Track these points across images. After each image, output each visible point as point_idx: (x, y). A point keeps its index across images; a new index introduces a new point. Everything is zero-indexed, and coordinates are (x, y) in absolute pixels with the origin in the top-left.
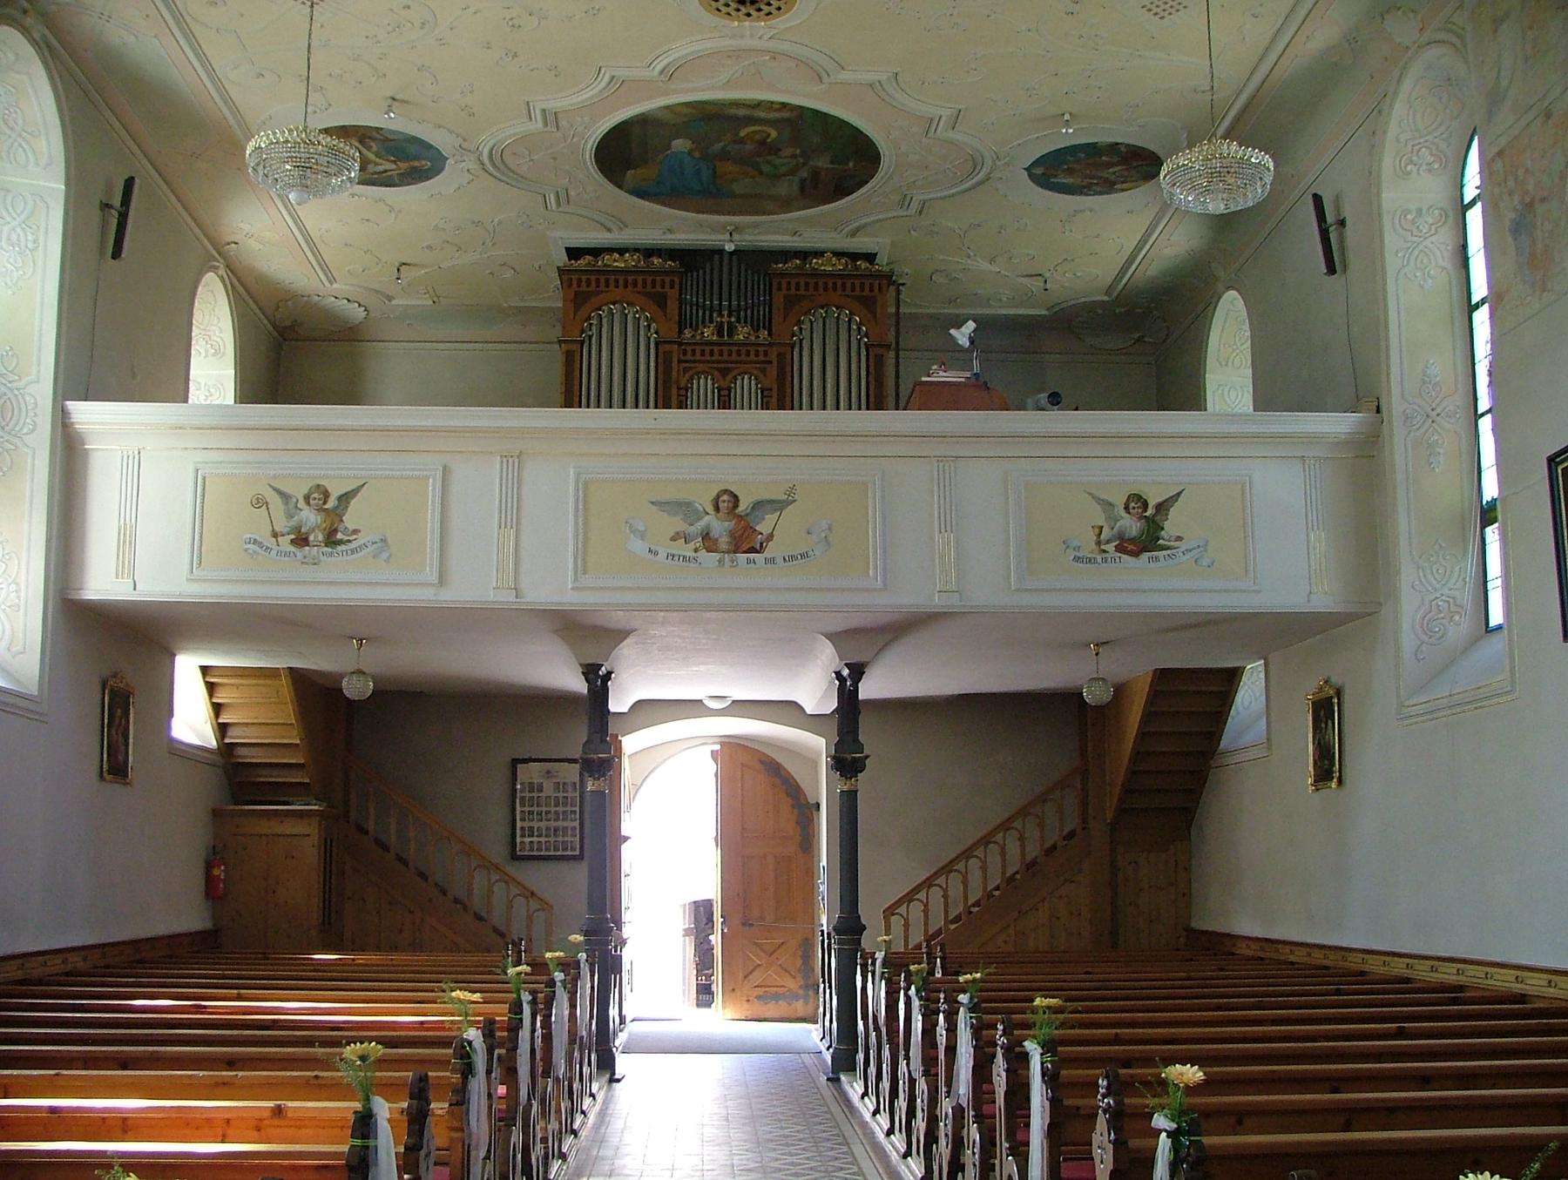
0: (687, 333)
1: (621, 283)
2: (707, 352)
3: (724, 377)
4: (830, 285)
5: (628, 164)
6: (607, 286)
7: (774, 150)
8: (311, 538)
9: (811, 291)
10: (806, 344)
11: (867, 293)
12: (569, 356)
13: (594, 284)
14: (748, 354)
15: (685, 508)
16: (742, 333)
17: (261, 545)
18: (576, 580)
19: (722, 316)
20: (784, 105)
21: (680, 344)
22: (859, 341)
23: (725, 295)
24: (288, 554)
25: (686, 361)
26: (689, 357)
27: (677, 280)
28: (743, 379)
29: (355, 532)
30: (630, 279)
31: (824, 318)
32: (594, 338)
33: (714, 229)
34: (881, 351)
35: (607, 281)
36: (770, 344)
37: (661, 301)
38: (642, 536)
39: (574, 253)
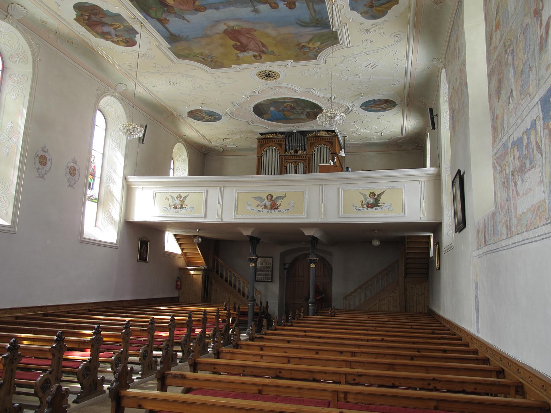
0: (287, 153)
1: (271, 141)
2: (291, 157)
3: (296, 163)
13: (265, 142)
14: (299, 157)
16: (300, 152)
19: (295, 148)
21: (285, 155)
22: (329, 152)
23: (296, 143)
25: (286, 160)
27: (284, 140)
28: (300, 163)
30: (273, 140)
31: (320, 147)
32: (265, 155)
35: (268, 141)
36: (307, 155)
37: (280, 145)
39: (261, 134)
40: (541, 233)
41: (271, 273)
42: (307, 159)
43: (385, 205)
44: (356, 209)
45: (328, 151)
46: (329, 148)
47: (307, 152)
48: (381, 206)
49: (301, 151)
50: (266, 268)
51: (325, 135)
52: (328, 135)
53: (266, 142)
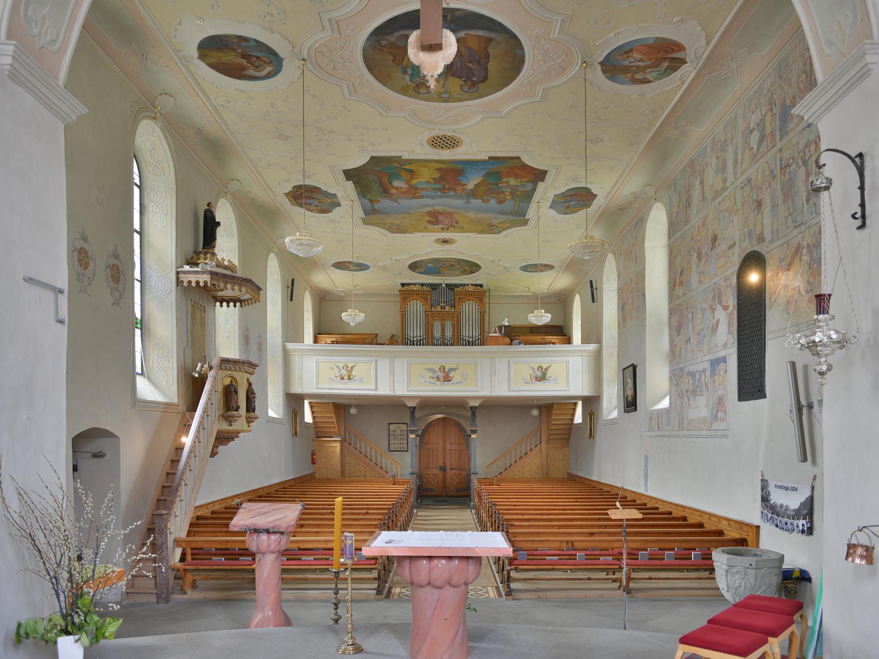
7: (453, 266)
8: (344, 378)
10: (464, 311)
15: (432, 370)
16: (447, 308)
18: (408, 388)
19: (442, 303)
20: (455, 259)
29: (355, 376)
34: (484, 313)
37: (426, 299)
38: (422, 377)
40: (704, 434)
42: (455, 317)
45: (477, 308)
46: (478, 305)
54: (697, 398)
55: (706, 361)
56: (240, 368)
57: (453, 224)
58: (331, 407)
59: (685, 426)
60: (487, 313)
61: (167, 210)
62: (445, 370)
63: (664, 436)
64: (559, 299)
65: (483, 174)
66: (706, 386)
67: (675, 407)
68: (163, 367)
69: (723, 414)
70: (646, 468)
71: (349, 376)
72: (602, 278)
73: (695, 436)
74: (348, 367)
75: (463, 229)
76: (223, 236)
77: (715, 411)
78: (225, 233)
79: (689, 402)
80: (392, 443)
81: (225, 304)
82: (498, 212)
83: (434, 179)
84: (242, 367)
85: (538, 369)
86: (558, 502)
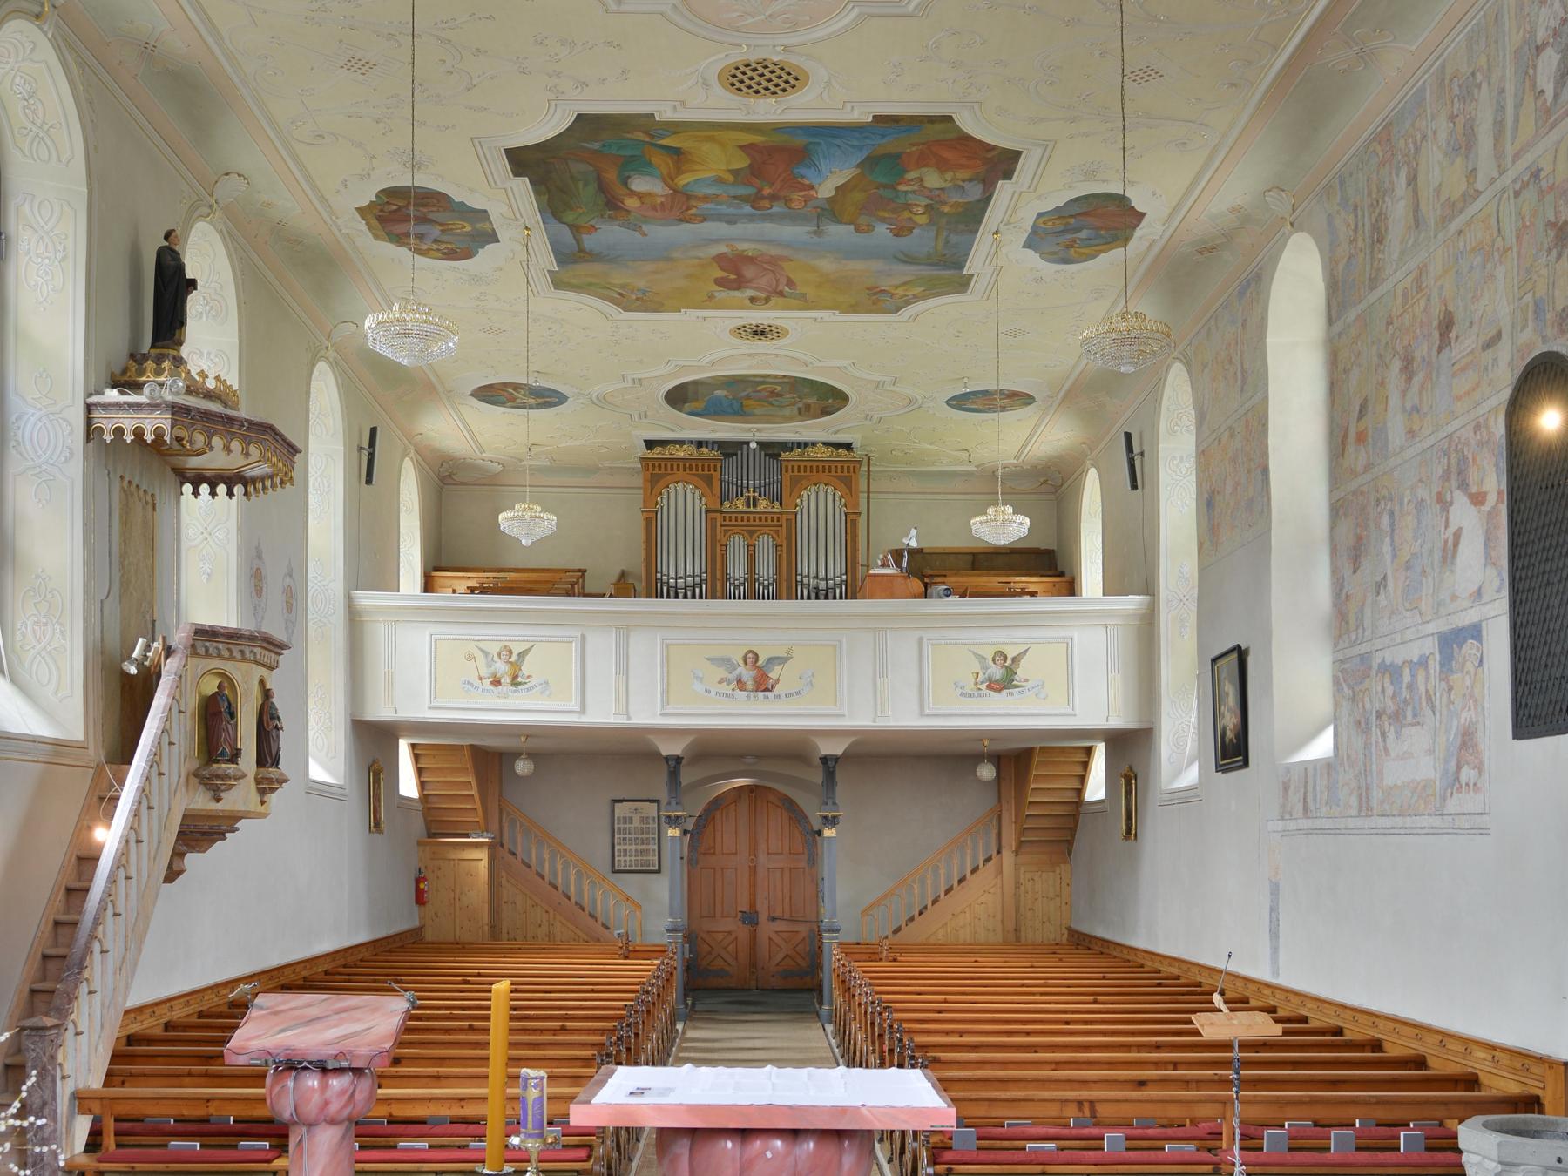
4: (821, 468)
5: (685, 401)
6: (672, 470)
7: (780, 395)
8: (502, 681)
9: (808, 473)
10: (805, 511)
11: (846, 473)
12: (648, 521)
14: (766, 520)
15: (726, 662)
16: (763, 504)
17: (472, 685)
18: (663, 708)
19: (748, 491)
20: (784, 376)
21: (721, 513)
23: (751, 477)
24: (488, 691)
26: (727, 522)
29: (529, 677)
33: (741, 430)
34: (854, 517)
36: (781, 513)
37: (708, 480)
38: (701, 680)
41: (656, 847)
43: (1029, 685)
44: (962, 695)
45: (837, 503)
46: (842, 496)
47: (781, 505)
48: (1019, 687)
49: (765, 502)
50: (642, 833)
51: (830, 456)
52: (839, 456)
53: (666, 470)
54: (1406, 731)
55: (1428, 635)
56: (242, 652)
57: (780, 288)
58: (466, 760)
59: (1375, 806)
60: (864, 517)
61: (64, 250)
62: (757, 661)
63: (1322, 831)
64: (1045, 482)
65: (859, 161)
66: (1429, 699)
67: (1348, 757)
68: (49, 649)
69: (1474, 773)
70: (1274, 916)
71: (516, 677)
72: (1154, 427)
73: (1402, 831)
74: (511, 652)
75: (805, 301)
76: (201, 318)
77: (1453, 764)
78: (208, 308)
79: (1384, 741)
80: (619, 850)
81: (204, 489)
82: (895, 257)
83: (735, 173)
84: (247, 650)
85: (994, 661)
86: (1049, 1003)
